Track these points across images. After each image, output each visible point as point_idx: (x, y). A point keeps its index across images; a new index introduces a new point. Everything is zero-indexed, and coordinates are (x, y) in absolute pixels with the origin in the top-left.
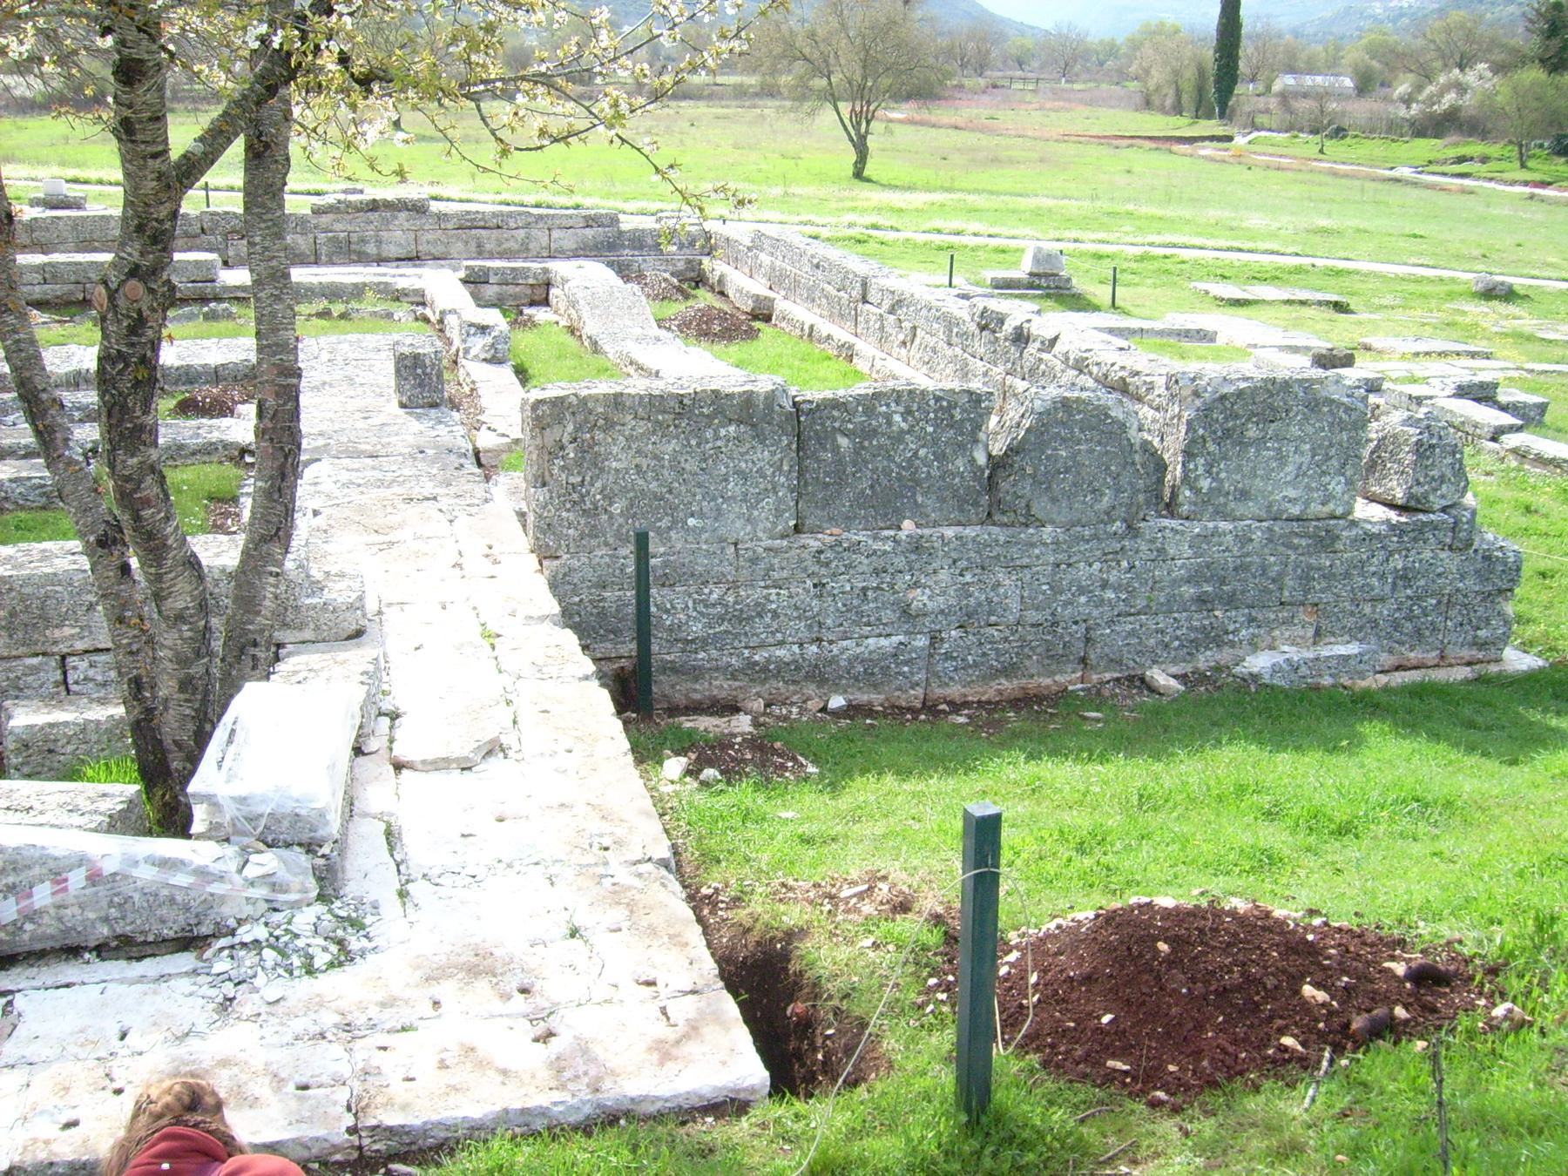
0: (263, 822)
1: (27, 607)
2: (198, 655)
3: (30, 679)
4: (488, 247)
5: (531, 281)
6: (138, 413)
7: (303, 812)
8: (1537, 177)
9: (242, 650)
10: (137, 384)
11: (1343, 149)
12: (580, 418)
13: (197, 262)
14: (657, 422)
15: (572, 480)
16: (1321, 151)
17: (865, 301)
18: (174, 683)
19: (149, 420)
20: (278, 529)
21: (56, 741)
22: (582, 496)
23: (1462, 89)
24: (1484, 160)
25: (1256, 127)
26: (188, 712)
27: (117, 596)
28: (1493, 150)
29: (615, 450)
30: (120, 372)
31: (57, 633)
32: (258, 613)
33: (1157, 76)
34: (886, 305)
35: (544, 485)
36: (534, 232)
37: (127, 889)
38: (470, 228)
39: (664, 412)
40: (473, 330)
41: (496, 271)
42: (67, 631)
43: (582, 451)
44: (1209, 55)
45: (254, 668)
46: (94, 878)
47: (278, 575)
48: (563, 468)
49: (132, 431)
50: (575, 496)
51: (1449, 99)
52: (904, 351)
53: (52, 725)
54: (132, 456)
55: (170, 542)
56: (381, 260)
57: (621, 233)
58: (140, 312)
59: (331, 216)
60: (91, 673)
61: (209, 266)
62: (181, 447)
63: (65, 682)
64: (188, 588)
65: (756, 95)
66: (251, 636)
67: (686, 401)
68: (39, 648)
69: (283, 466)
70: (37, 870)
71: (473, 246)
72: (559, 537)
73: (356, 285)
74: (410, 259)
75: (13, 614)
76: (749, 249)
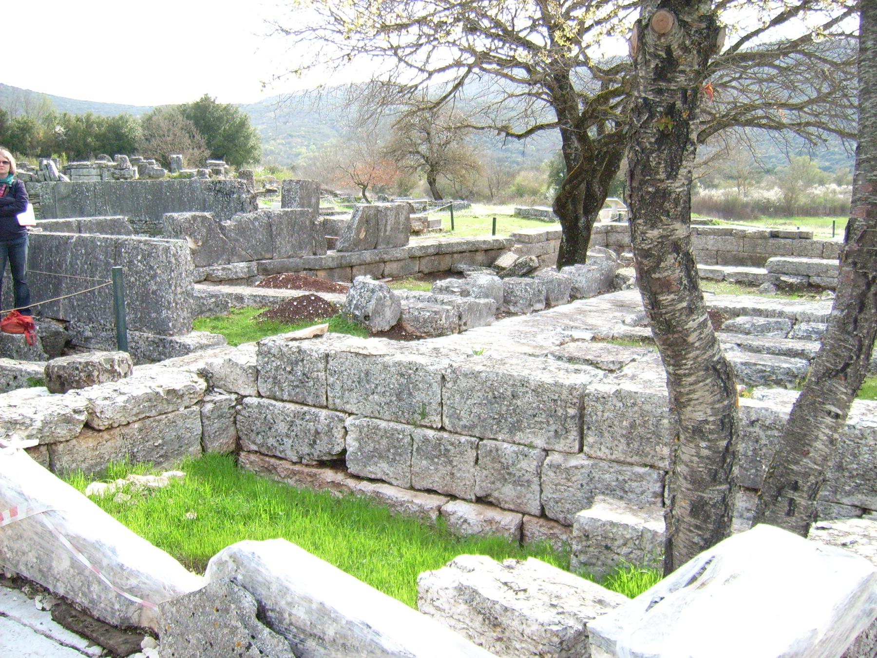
1: (645, 422)
2: (714, 479)
3: (634, 484)
6: (662, 176)
9: (780, 491)
10: (663, 137)
19: (677, 186)
20: (847, 365)
21: (614, 539)
26: (696, 539)
32: (806, 454)
45: (790, 513)
47: (837, 416)
49: (653, 196)
53: (612, 524)
54: (653, 226)
55: (692, 338)
58: (669, 50)
64: (709, 398)
66: (793, 478)
68: (648, 460)
69: (864, 295)
75: (633, 426)
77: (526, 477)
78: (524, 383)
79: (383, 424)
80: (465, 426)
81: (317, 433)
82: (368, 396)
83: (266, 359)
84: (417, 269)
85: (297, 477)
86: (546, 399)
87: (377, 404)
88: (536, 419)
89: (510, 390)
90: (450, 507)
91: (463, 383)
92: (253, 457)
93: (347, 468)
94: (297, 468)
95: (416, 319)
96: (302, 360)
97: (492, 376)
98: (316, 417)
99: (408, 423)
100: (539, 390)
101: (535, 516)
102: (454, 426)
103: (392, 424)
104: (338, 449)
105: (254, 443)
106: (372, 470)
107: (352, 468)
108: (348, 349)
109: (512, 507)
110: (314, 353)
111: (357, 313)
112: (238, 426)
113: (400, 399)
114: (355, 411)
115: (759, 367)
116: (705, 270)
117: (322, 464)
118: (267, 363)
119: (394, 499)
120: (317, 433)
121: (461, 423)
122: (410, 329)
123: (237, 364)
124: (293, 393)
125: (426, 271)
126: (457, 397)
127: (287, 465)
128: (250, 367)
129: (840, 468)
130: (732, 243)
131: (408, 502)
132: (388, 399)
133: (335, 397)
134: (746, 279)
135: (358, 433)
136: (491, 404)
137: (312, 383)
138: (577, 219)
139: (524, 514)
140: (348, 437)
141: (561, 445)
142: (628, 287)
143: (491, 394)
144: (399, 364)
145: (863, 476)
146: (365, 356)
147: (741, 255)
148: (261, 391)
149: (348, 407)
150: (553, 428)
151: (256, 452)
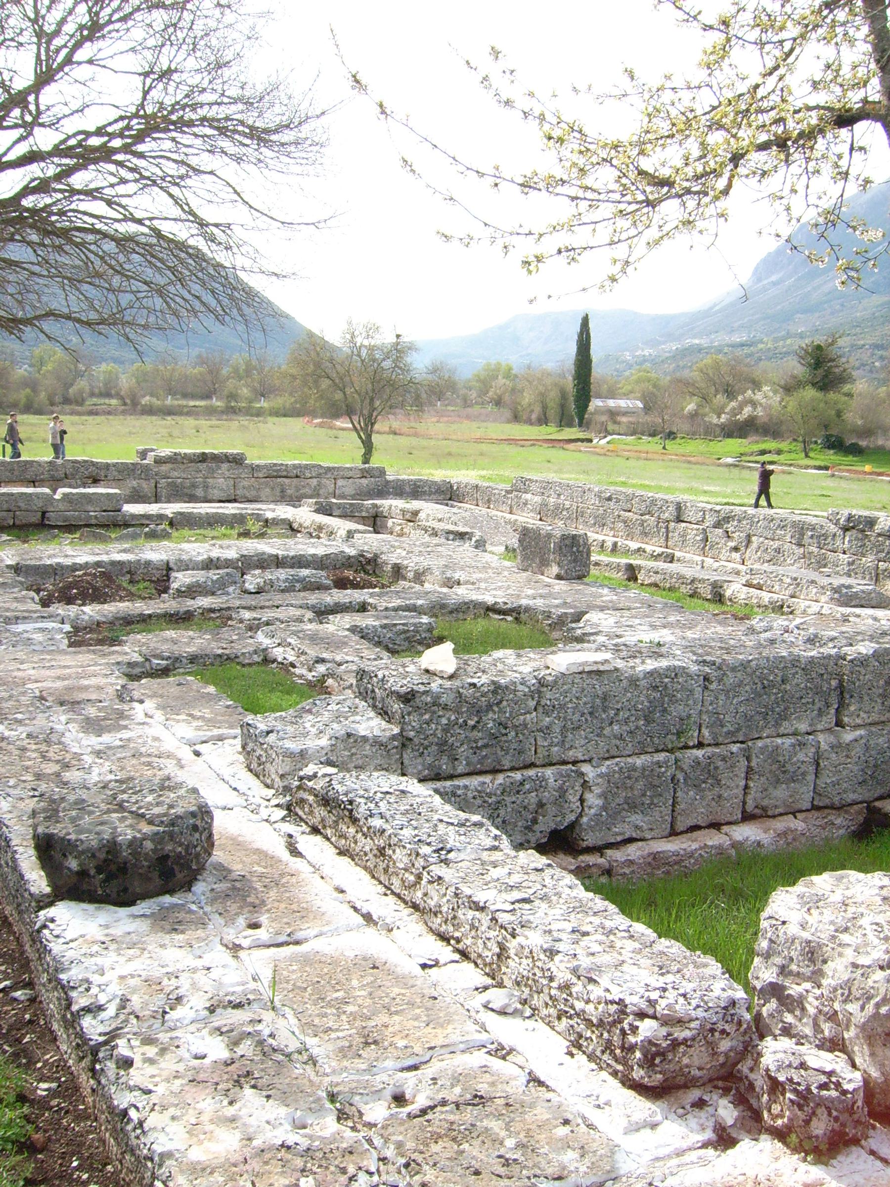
4: (289, 492)
5: (364, 514)
8: (817, 463)
11: (676, 446)
13: (108, 494)
16: (664, 448)
23: (754, 404)
24: (779, 452)
25: (608, 433)
28: (784, 445)
33: (527, 398)
34: (710, 521)
36: (324, 481)
38: (276, 477)
40: (451, 537)
44: (569, 382)
51: (747, 411)
52: (736, 556)
57: (388, 482)
59: (169, 466)
65: (223, 412)
71: (278, 492)
76: (508, 492)
80: (729, 733)
81: (541, 805)
82: (602, 728)
83: (427, 717)
87: (615, 737)
88: (803, 701)
91: (731, 679)
97: (763, 662)
98: (540, 784)
99: (657, 751)
101: (808, 810)
102: (714, 735)
104: (573, 817)
106: (623, 829)
107: (590, 839)
108: (581, 669)
109: (781, 810)
110: (520, 688)
113: (648, 720)
115: (401, 627)
119: (682, 852)
121: (725, 730)
123: (365, 739)
124: (475, 759)
131: (701, 848)
132: (632, 726)
135: (606, 785)
137: (513, 733)
143: (759, 685)
144: (651, 673)
146: (599, 673)
150: (816, 707)
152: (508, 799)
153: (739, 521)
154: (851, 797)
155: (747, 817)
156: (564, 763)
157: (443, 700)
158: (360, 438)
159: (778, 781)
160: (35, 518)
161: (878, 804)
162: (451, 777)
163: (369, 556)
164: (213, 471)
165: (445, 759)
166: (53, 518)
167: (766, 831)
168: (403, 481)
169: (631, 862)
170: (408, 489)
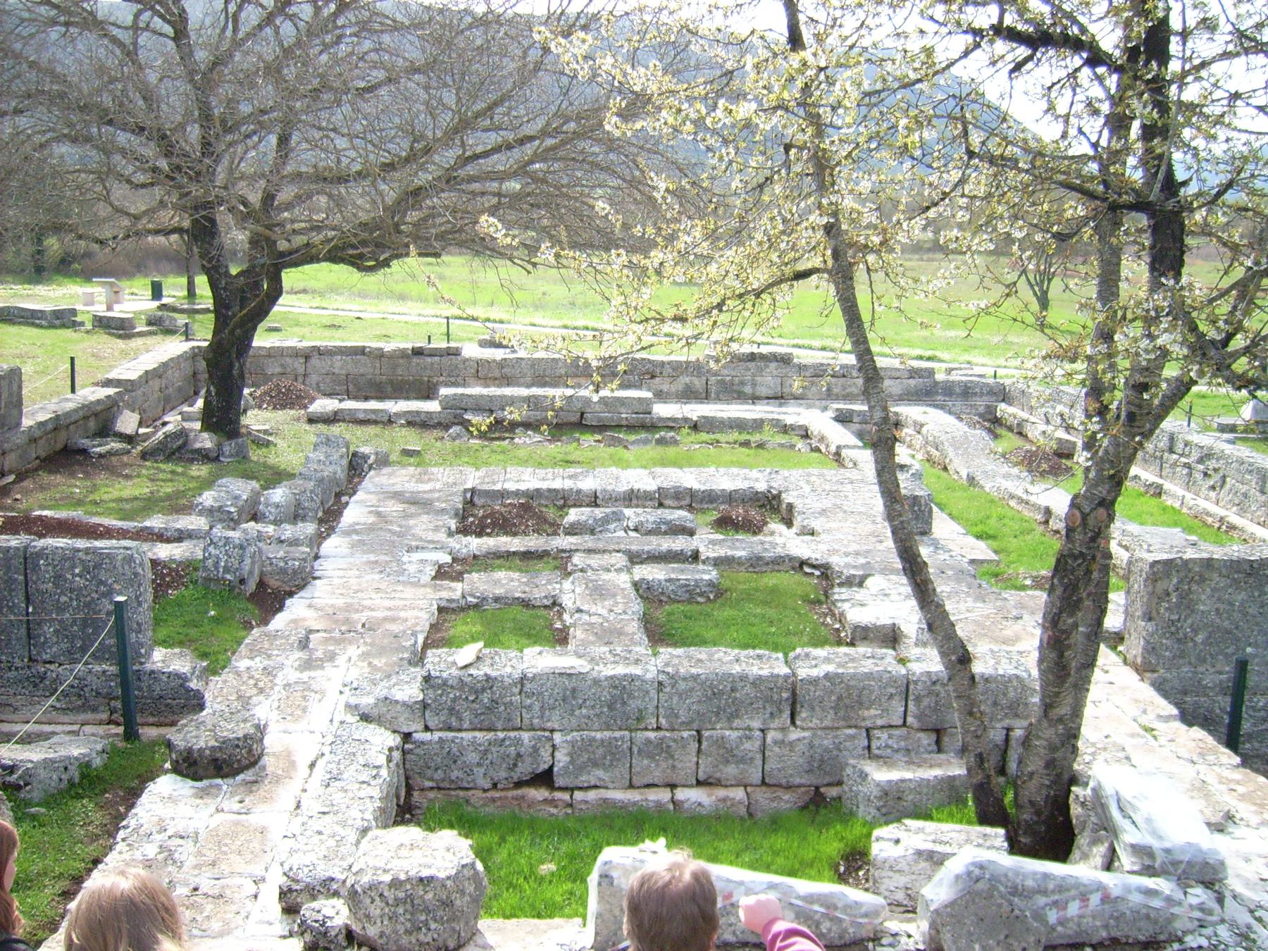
0: (1183, 866)
3: (848, 744)
4: (835, 391)
7: (1211, 861)
12: (1182, 574)
14: (1234, 579)
15: (1173, 617)
17: (1171, 451)
18: (1042, 763)
22: (1178, 629)
26: (1047, 782)
27: (969, 697)
29: (1203, 597)
30: (1079, 565)
31: (866, 713)
34: (1195, 455)
35: (1150, 619)
37: (1122, 907)
39: (1238, 572)
41: (860, 413)
42: (873, 712)
43: (1181, 597)
46: (1106, 898)
48: (1167, 609)
50: (1173, 629)
52: (1212, 494)
53: (903, 781)
56: (755, 399)
57: (936, 383)
60: (890, 742)
61: (648, 402)
62: (759, 558)
63: (869, 747)
65: (929, 250)
67: (1255, 565)
68: (850, 723)
70: (1073, 892)
72: (1159, 656)
73: (755, 420)
74: (776, 398)
75: (840, 698)
77: (750, 755)
78: (743, 678)
79: (599, 735)
81: (519, 755)
84: (34, 456)
85: (499, 803)
86: (763, 688)
89: (729, 686)
90: (681, 794)
91: (682, 686)
92: (432, 795)
93: (553, 782)
94: (497, 794)
95: (283, 571)
96: (491, 688)
98: (518, 742)
99: (620, 729)
100: (758, 682)
103: (607, 734)
104: (546, 767)
105: (432, 779)
106: (584, 779)
107: (559, 781)
110: (506, 679)
111: (228, 577)
112: (407, 766)
113: (611, 707)
114: (556, 726)
116: (365, 411)
117: (519, 784)
118: (441, 696)
120: (519, 755)
122: (273, 583)
123: (397, 702)
125: (43, 455)
126: (675, 700)
127: (480, 794)
128: (416, 702)
129: (995, 704)
130: (365, 365)
133: (533, 717)
134: (417, 419)
136: (710, 699)
138: (231, 365)
139: (745, 787)
140: (557, 754)
141: (776, 723)
142: (370, 468)
144: (612, 677)
145: (1010, 708)
147: (378, 379)
148: (430, 724)
149: (549, 725)
150: (769, 710)
151: (432, 788)
152: (493, 749)
153: (1218, 460)
154: (798, 781)
155: (699, 783)
156: (544, 730)
157: (450, 682)
158: (1035, 294)
159: (728, 761)
160: (574, 418)
161: (822, 790)
162: (460, 730)
163: (774, 492)
164: (762, 370)
165: (453, 719)
166: (590, 419)
167: (710, 795)
168: (953, 382)
169: (586, 802)
170: (958, 390)
